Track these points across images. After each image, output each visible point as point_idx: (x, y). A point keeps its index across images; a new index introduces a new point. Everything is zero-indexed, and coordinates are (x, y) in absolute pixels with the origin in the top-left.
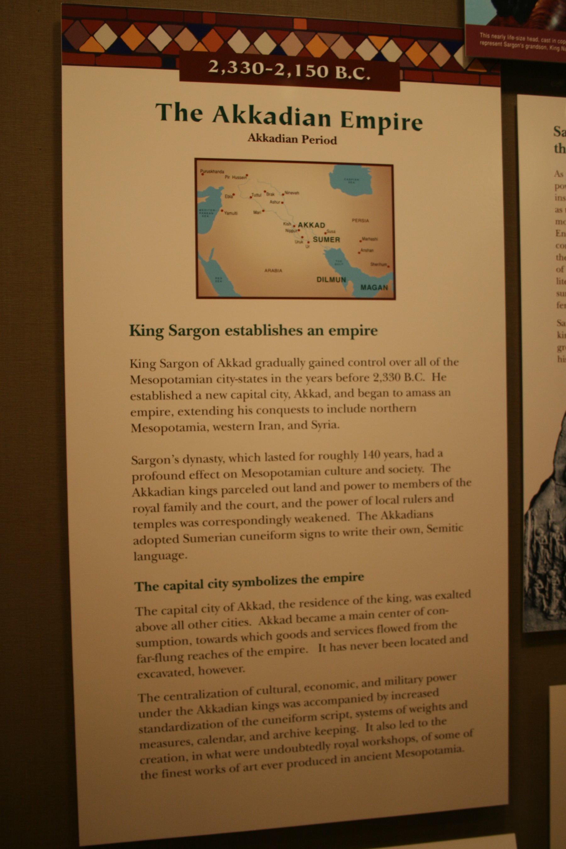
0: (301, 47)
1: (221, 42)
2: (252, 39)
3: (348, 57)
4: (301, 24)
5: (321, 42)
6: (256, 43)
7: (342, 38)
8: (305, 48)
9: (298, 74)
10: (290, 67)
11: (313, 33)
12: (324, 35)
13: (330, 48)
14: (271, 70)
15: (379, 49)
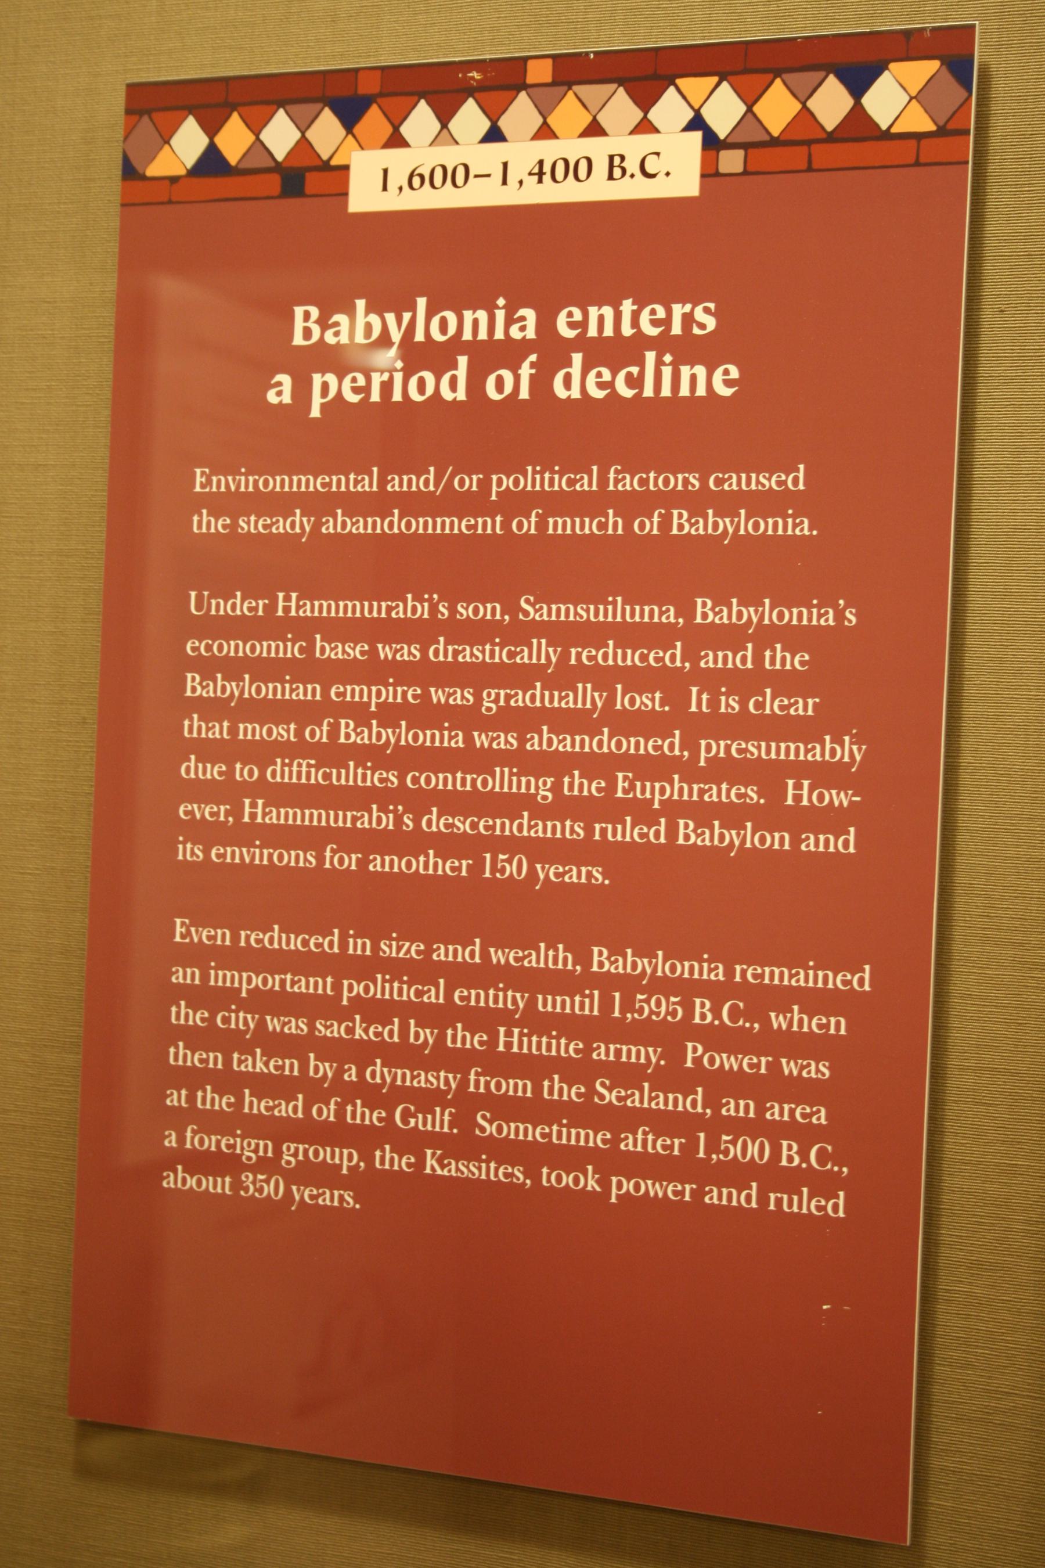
4: (540, 72)
7: (621, 90)
11: (565, 88)
15: (696, 107)
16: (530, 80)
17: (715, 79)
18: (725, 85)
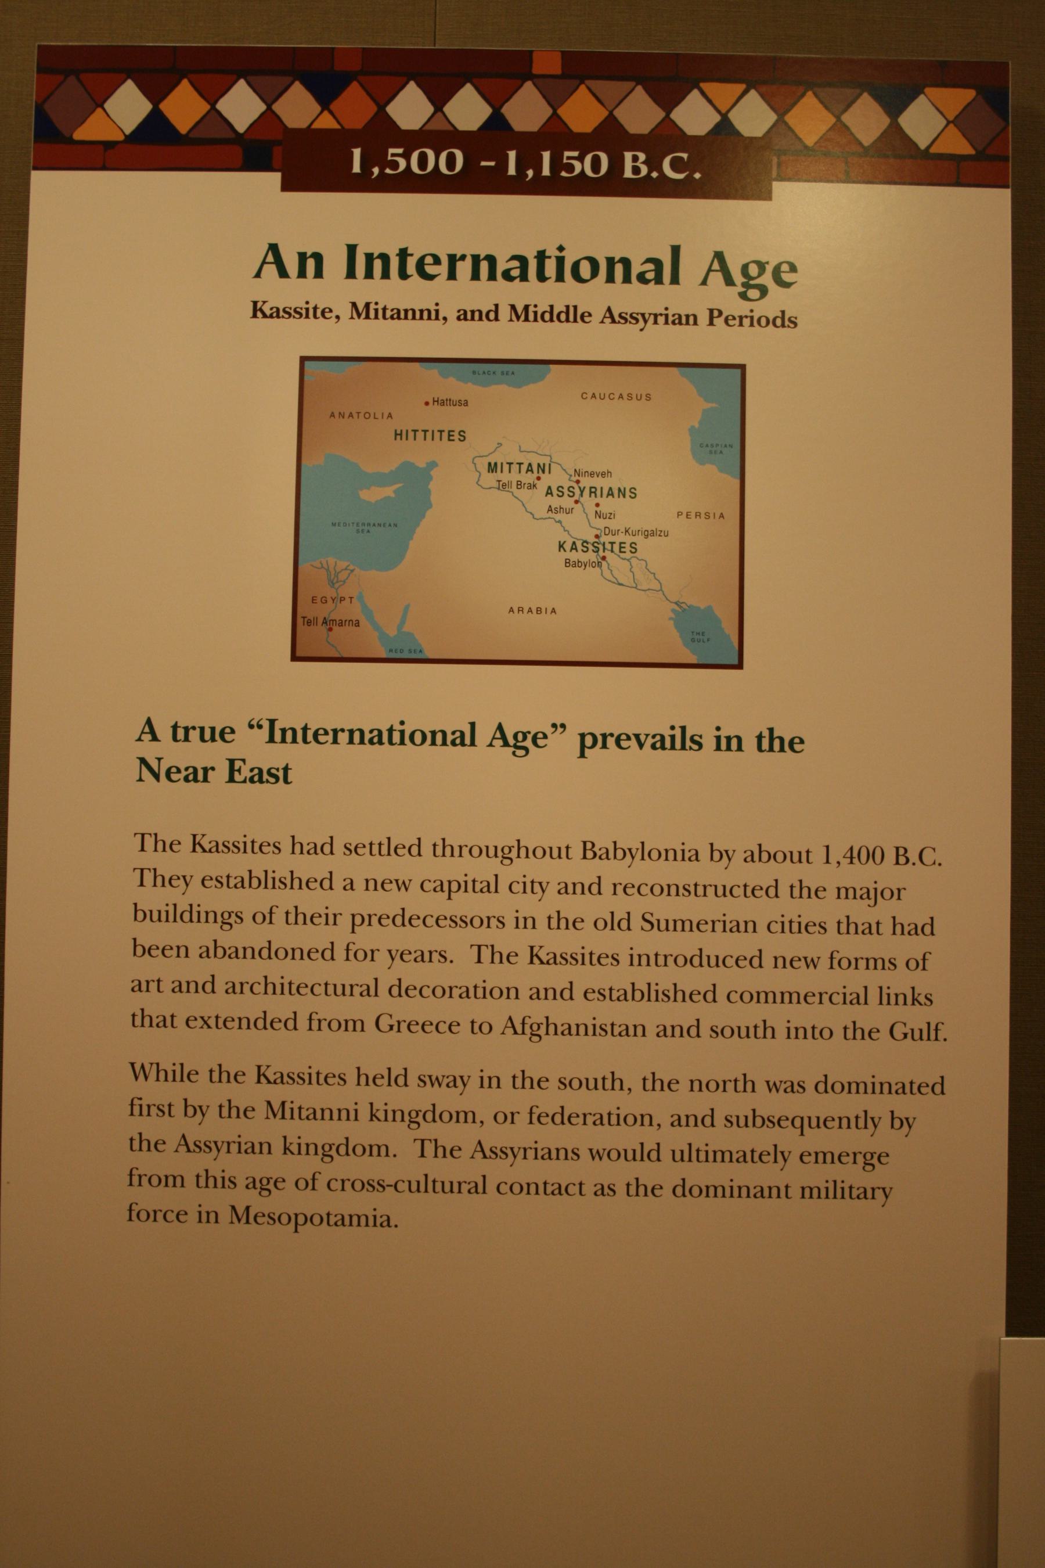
0: (549, 112)
1: (373, 109)
2: (439, 98)
3: (653, 130)
4: (547, 63)
5: (593, 99)
6: (446, 109)
7: (639, 89)
8: (555, 115)
9: (546, 171)
11: (578, 82)
12: (597, 85)
13: (611, 113)
15: (724, 111)
16: (536, 71)
17: (743, 86)
18: (753, 93)
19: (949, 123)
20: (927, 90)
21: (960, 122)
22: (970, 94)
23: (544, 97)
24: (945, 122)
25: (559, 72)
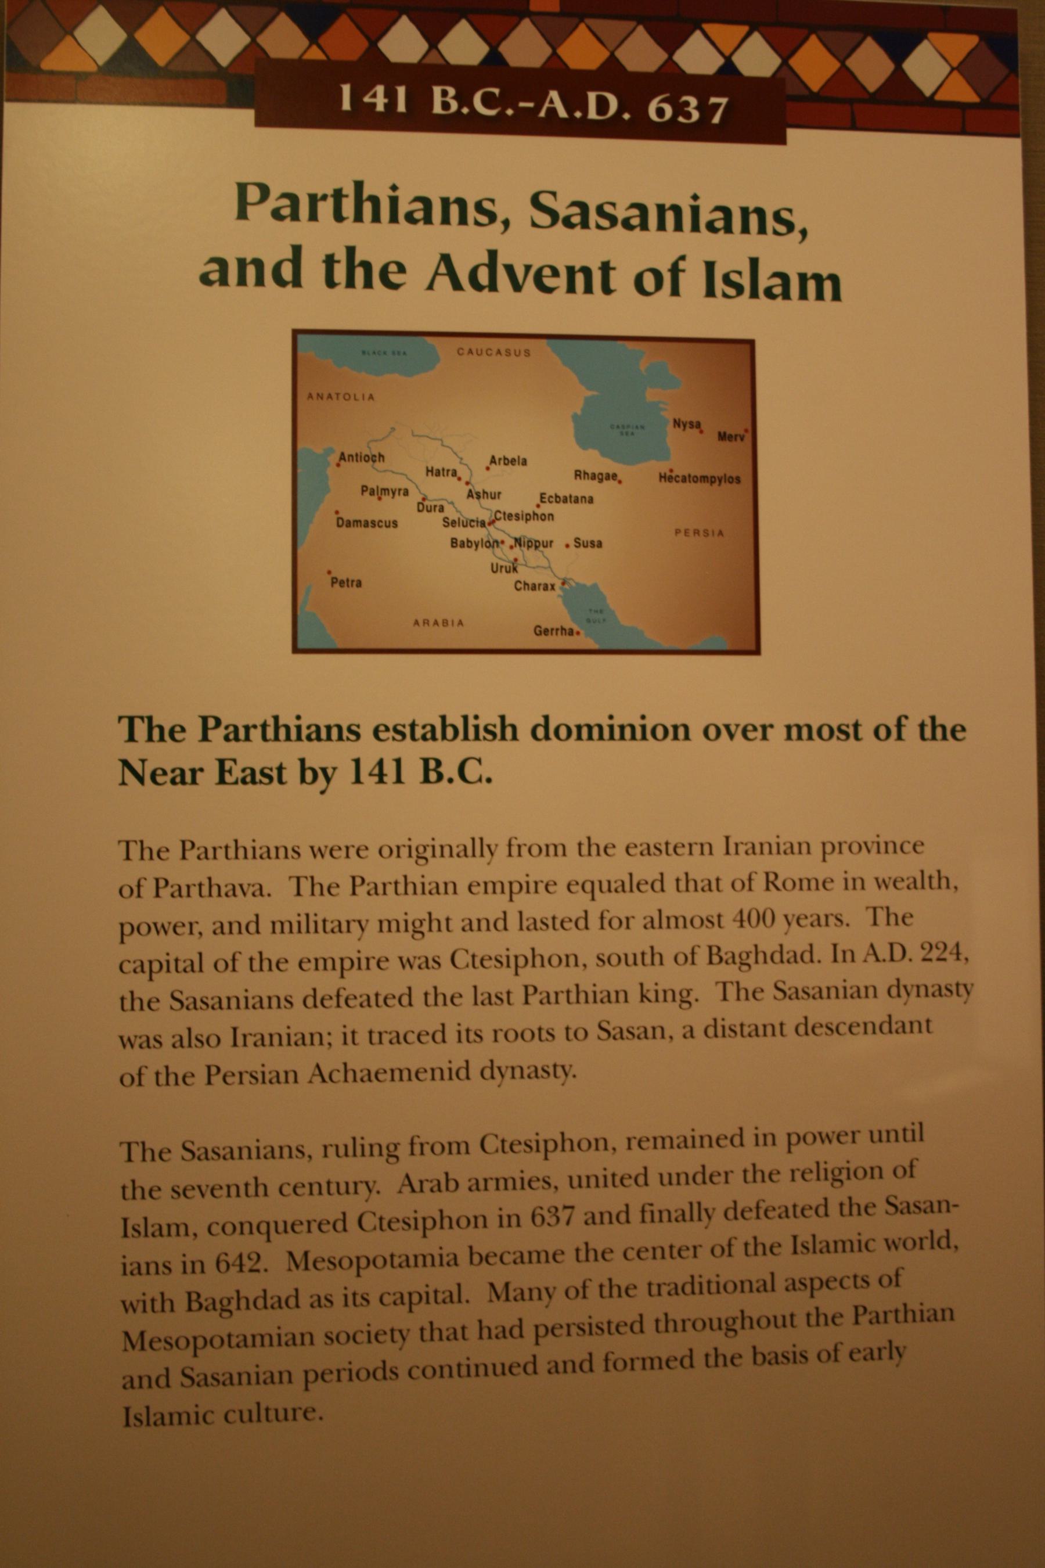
0: (548, 51)
1: (364, 44)
2: (433, 36)
6: (444, 46)
7: (641, 29)
8: (554, 54)
10: (574, 101)
12: (597, 24)
13: (612, 55)
14: (531, 105)
15: (727, 54)
16: (534, 7)
18: (756, 37)
19: (953, 69)
20: (931, 35)
21: (963, 68)
22: (972, 40)
23: (543, 35)
24: (948, 69)
25: (556, 8)
